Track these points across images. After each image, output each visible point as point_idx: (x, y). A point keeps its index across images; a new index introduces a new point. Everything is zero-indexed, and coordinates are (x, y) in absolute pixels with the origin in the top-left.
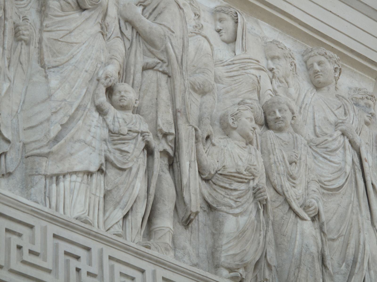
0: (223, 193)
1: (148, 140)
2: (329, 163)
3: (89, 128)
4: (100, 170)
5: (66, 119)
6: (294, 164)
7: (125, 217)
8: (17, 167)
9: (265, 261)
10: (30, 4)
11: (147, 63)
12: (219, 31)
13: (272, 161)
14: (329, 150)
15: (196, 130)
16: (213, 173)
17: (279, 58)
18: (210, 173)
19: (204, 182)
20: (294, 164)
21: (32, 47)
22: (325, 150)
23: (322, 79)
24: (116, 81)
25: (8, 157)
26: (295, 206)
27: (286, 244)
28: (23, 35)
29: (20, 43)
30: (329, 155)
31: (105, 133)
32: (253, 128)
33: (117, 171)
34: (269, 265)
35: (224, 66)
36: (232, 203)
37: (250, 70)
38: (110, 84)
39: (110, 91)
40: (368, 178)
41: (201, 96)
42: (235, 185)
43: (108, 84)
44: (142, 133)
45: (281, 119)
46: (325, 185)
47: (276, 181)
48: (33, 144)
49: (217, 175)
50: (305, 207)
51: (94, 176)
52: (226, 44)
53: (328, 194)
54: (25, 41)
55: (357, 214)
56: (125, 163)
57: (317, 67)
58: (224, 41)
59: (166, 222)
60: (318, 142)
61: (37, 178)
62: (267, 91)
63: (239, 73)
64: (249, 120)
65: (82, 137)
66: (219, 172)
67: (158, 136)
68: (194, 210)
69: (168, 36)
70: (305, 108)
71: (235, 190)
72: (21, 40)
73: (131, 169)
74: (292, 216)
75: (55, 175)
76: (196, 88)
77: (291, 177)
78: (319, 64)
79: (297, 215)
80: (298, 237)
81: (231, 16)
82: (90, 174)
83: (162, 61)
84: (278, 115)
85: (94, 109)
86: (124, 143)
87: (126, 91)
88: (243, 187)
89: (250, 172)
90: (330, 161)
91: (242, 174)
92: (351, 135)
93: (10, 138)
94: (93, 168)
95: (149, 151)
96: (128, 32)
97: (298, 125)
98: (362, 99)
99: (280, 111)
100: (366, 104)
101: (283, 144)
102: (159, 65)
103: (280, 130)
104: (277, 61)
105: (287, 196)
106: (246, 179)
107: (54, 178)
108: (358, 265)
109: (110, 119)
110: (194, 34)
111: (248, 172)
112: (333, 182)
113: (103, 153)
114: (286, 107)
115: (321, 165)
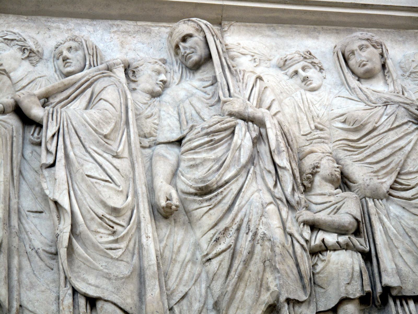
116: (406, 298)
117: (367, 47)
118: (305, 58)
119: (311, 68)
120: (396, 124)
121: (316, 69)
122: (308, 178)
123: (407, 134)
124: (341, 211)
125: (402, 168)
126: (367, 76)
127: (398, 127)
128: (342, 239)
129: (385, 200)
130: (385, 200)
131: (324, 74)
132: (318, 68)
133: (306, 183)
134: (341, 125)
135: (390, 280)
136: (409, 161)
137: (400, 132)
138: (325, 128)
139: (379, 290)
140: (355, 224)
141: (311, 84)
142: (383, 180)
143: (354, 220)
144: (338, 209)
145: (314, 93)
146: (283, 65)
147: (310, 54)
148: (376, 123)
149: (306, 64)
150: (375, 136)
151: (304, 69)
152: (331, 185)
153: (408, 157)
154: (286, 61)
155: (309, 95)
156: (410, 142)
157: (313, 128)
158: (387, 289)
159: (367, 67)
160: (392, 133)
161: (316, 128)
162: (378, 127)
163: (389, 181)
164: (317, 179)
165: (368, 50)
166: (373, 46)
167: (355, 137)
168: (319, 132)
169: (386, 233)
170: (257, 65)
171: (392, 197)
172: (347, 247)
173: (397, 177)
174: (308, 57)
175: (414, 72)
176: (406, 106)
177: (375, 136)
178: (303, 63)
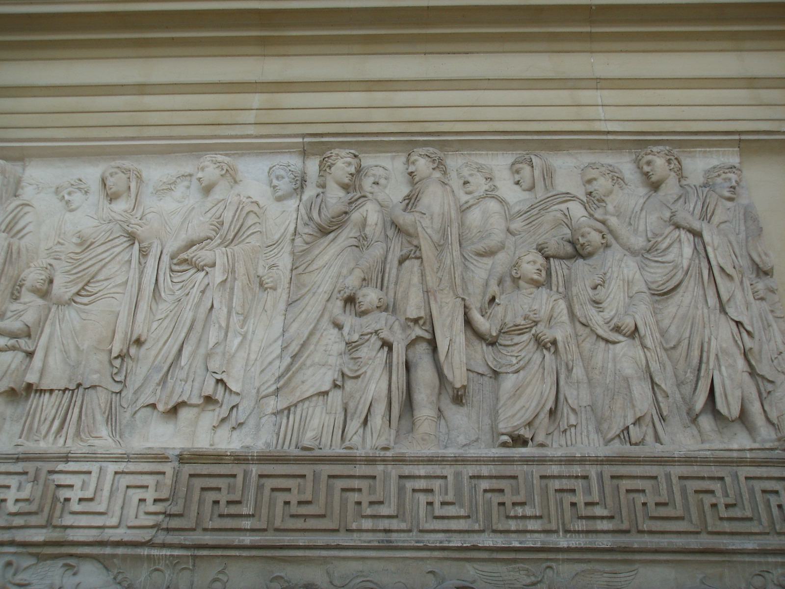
0: (505, 352)
1: (382, 335)
2: (662, 265)
3: (324, 348)
4: (336, 386)
5: (297, 349)
6: (599, 286)
7: (365, 422)
8: (249, 415)
9: (568, 406)
10: (283, 250)
11: (402, 255)
12: (517, 183)
13: (574, 292)
14: (659, 251)
15: (463, 299)
16: (494, 334)
17: (595, 179)
18: (491, 336)
19: (490, 347)
20: (599, 286)
21: (279, 290)
22: (656, 253)
23: (654, 178)
24: (355, 289)
25: (241, 408)
26: (600, 332)
27: (598, 377)
28: (267, 283)
29: (266, 292)
30: (660, 257)
31: (342, 346)
32: (538, 270)
33: (353, 380)
34: (573, 410)
35: (521, 216)
36: (514, 361)
37: (552, 208)
38: (345, 295)
39: (350, 301)
40: (713, 263)
41: (492, 257)
42: (517, 339)
43: (342, 297)
44: (376, 332)
45: (586, 244)
46: (658, 291)
47: (578, 313)
48: (262, 387)
49: (502, 334)
50: (617, 329)
51: (331, 394)
52: (527, 192)
53: (663, 299)
54: (271, 288)
55: (703, 308)
56: (357, 371)
57: (646, 169)
58: (524, 190)
59: (425, 411)
60: (648, 248)
61: (263, 420)
62: (579, 218)
63: (539, 215)
64: (532, 263)
65: (317, 360)
66: (502, 331)
67: (409, 326)
68: (458, 385)
69: (419, 221)
70: (635, 217)
71: (517, 344)
72: (266, 289)
73: (366, 372)
74: (602, 344)
75: (285, 409)
76: (481, 253)
77: (596, 303)
78: (649, 163)
79: (607, 341)
80: (610, 365)
81: (526, 163)
82: (326, 393)
83: (416, 246)
84: (581, 241)
85: (331, 326)
86: (357, 350)
87: (364, 296)
88: (525, 337)
89: (531, 320)
90: (663, 263)
91: (519, 325)
92: (686, 225)
93: (238, 391)
94: (325, 388)
95: (387, 345)
96: (391, 232)
97: (623, 239)
98: (719, 175)
99: (583, 236)
100: (725, 179)
101: (591, 270)
102: (413, 252)
103: (590, 255)
104: (595, 182)
105: (591, 325)
106: (526, 328)
107: (286, 412)
108: (704, 366)
109: (346, 330)
110: (481, 199)
111: (527, 321)
112: (667, 284)
113: (337, 369)
114: (588, 229)
115: (652, 271)
116: (45, 391)
117: (116, 173)
118: (72, 185)
119: (76, 192)
120: (111, 238)
121: (82, 192)
122: (17, 289)
123: (114, 247)
124: (21, 318)
125: (93, 278)
126: (112, 198)
127: (109, 241)
128: (12, 342)
129: (67, 305)
130: (67, 305)
131: (87, 196)
132: (83, 191)
133: (16, 293)
134: (74, 240)
135: (32, 378)
136: (104, 269)
137: (108, 245)
138: (65, 243)
139: (24, 385)
140: (26, 329)
141: (71, 206)
142: (70, 289)
143: (25, 326)
144: (20, 316)
145: (72, 213)
146: (57, 191)
147: (81, 181)
148: (94, 239)
149: (73, 189)
150: (91, 250)
151: (69, 194)
152: (33, 294)
153: (104, 266)
154: (58, 188)
155: (68, 215)
156: (112, 254)
157: (56, 242)
158: (29, 386)
159: (112, 190)
160: (104, 245)
161: (59, 243)
162: (95, 242)
163: (75, 290)
164: (24, 289)
165: (117, 176)
166: (123, 172)
167: (78, 250)
168: (60, 246)
169: (51, 336)
170: (38, 193)
171: (73, 303)
172: (13, 348)
173: (86, 285)
174: (74, 184)
175: (160, 190)
176: (120, 222)
177: (91, 250)
178: (71, 189)
